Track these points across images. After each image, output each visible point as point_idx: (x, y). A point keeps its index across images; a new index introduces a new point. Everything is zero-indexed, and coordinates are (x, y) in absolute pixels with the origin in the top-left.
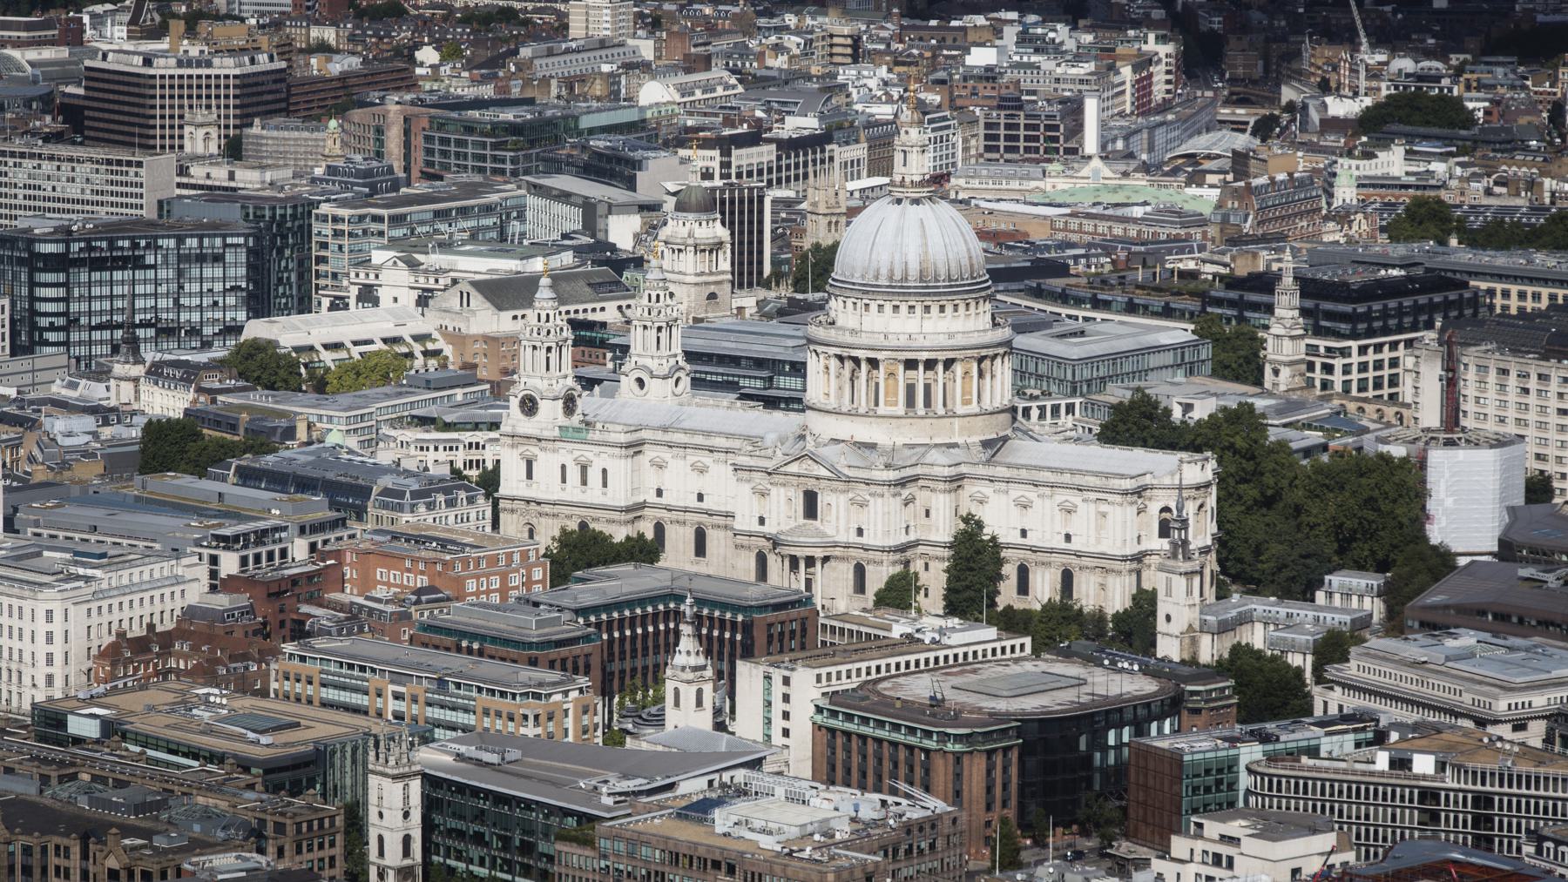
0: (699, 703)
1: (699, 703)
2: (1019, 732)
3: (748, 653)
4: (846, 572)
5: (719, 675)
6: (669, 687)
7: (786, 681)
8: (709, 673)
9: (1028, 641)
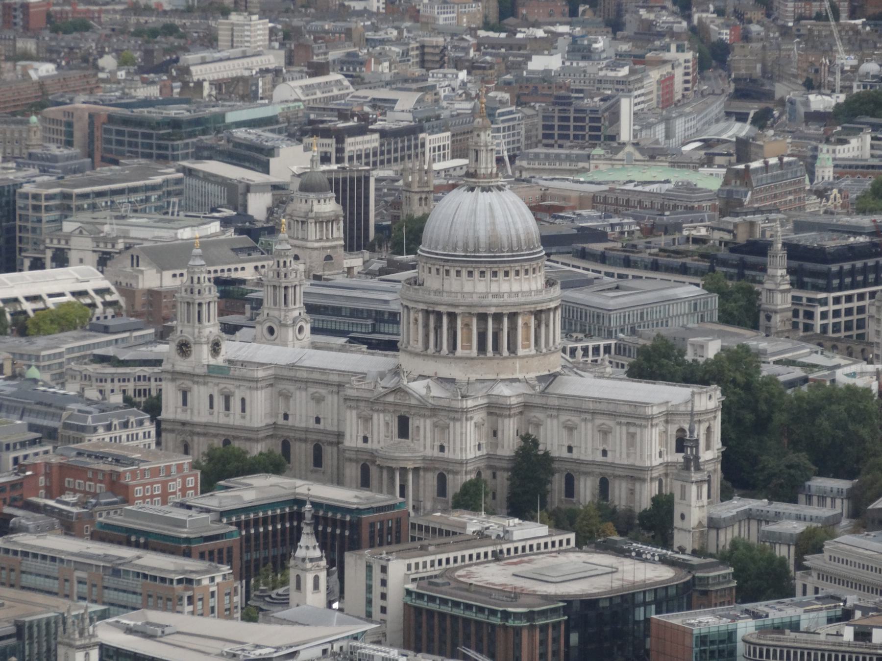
0: (316, 587)
1: (316, 587)
2: (566, 610)
3: (355, 545)
4: (430, 481)
5: (331, 563)
6: (292, 574)
7: (384, 569)
8: (324, 563)
9: (572, 536)
